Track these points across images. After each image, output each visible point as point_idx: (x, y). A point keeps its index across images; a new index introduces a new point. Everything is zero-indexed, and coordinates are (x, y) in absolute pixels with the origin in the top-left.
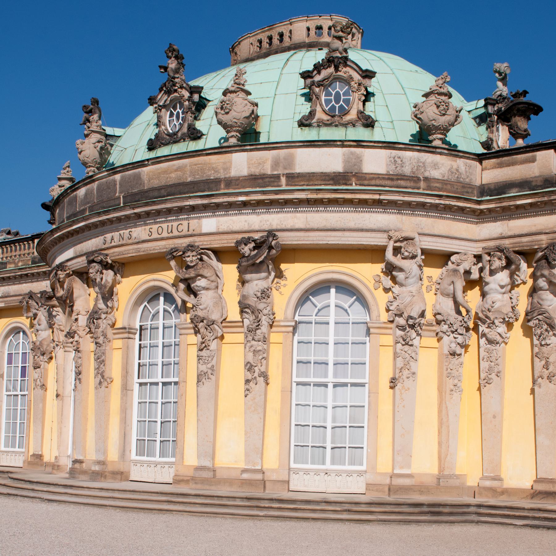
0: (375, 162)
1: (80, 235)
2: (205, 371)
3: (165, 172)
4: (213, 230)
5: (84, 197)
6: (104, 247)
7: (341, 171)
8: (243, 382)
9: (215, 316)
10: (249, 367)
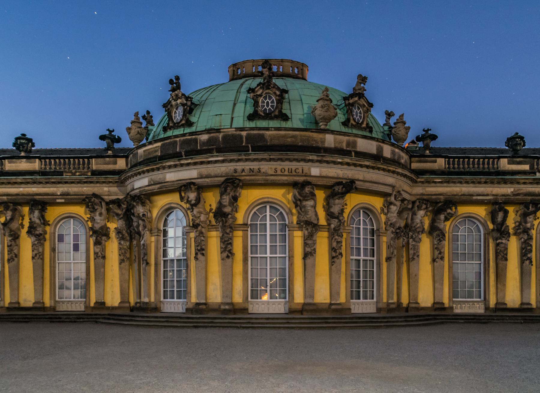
0: (387, 151)
4: (318, 174)
7: (375, 153)
9: (315, 222)
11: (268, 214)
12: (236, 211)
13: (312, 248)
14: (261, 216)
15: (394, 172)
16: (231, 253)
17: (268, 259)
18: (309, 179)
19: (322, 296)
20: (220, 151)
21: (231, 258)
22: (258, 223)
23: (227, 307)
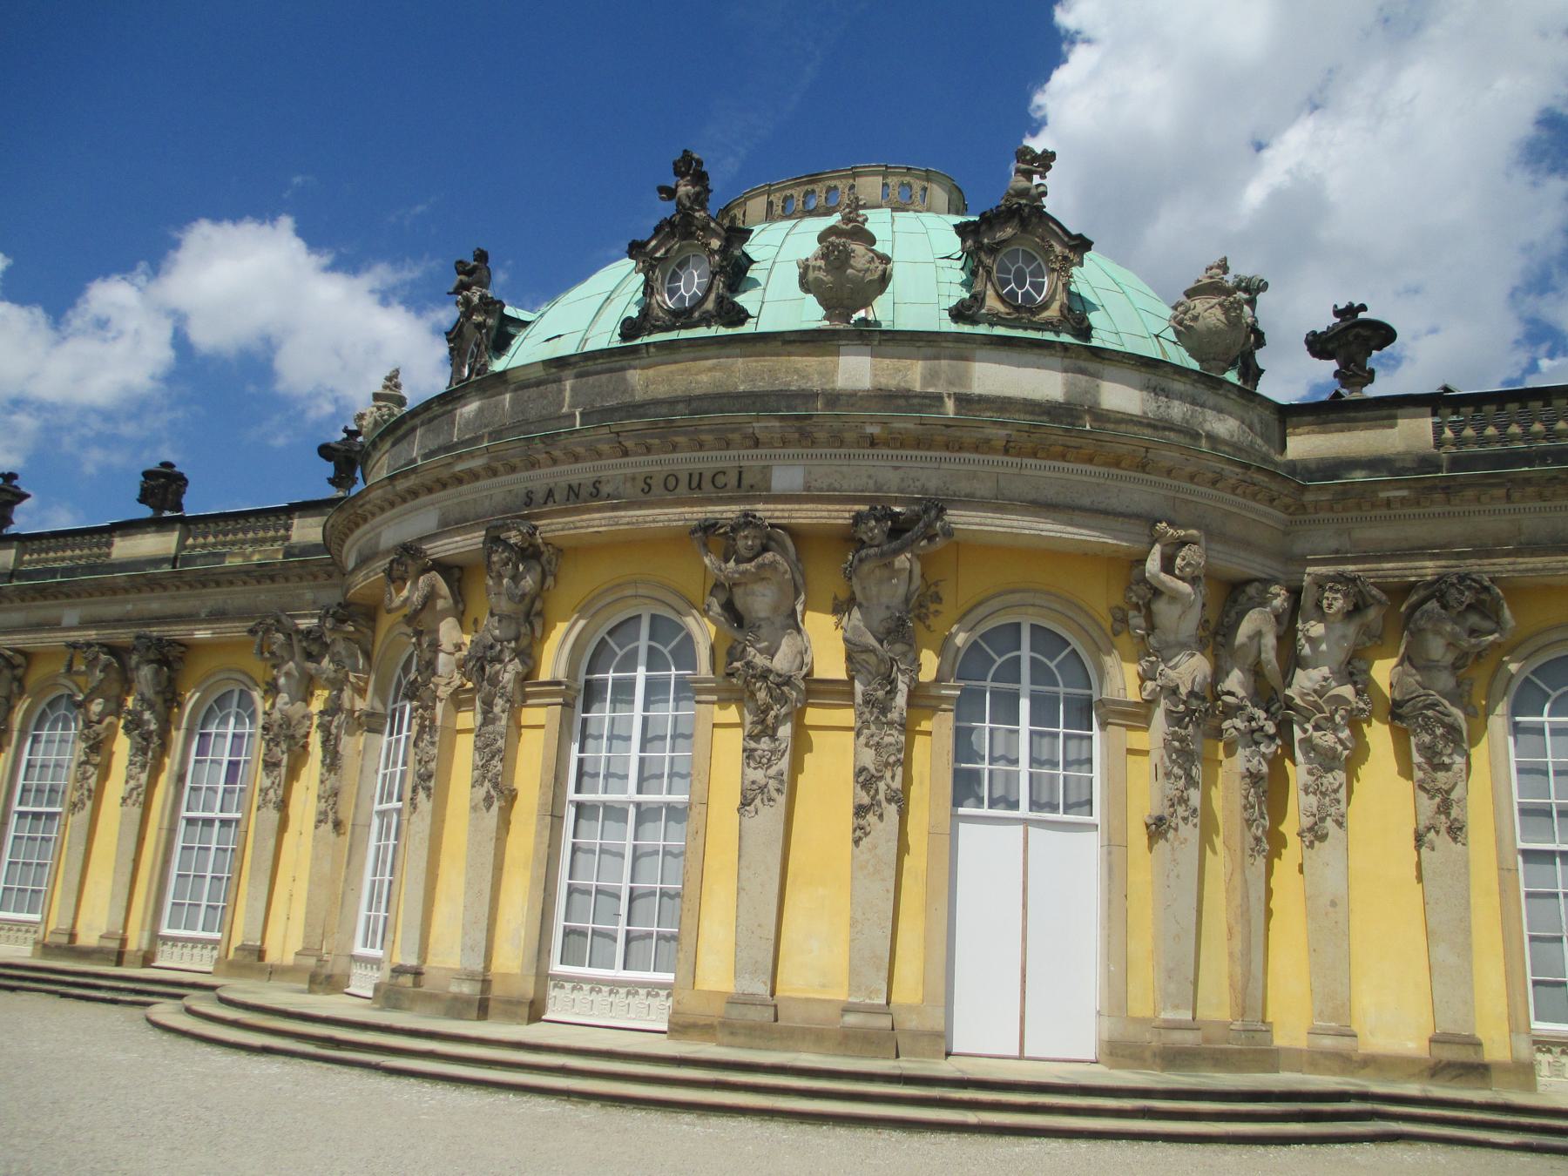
2: (763, 782)
7: (1061, 400)
8: (851, 810)
10: (866, 780)
11: (643, 643)
13: (772, 771)
15: (1143, 467)
16: (496, 786)
23: (466, 989)
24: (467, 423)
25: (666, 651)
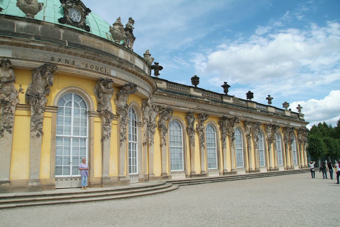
1: (28, 49)
3: (92, 42)
4: (115, 75)
5: (26, 28)
6: (53, 62)
10: (121, 134)
12: (48, 95)
13: (108, 132)
14: (67, 102)
17: (72, 139)
18: (110, 78)
19: (113, 172)
20: (38, 38)
21: (41, 136)
22: (65, 107)
23: (35, 184)
24: (21, 28)
25: (78, 103)
